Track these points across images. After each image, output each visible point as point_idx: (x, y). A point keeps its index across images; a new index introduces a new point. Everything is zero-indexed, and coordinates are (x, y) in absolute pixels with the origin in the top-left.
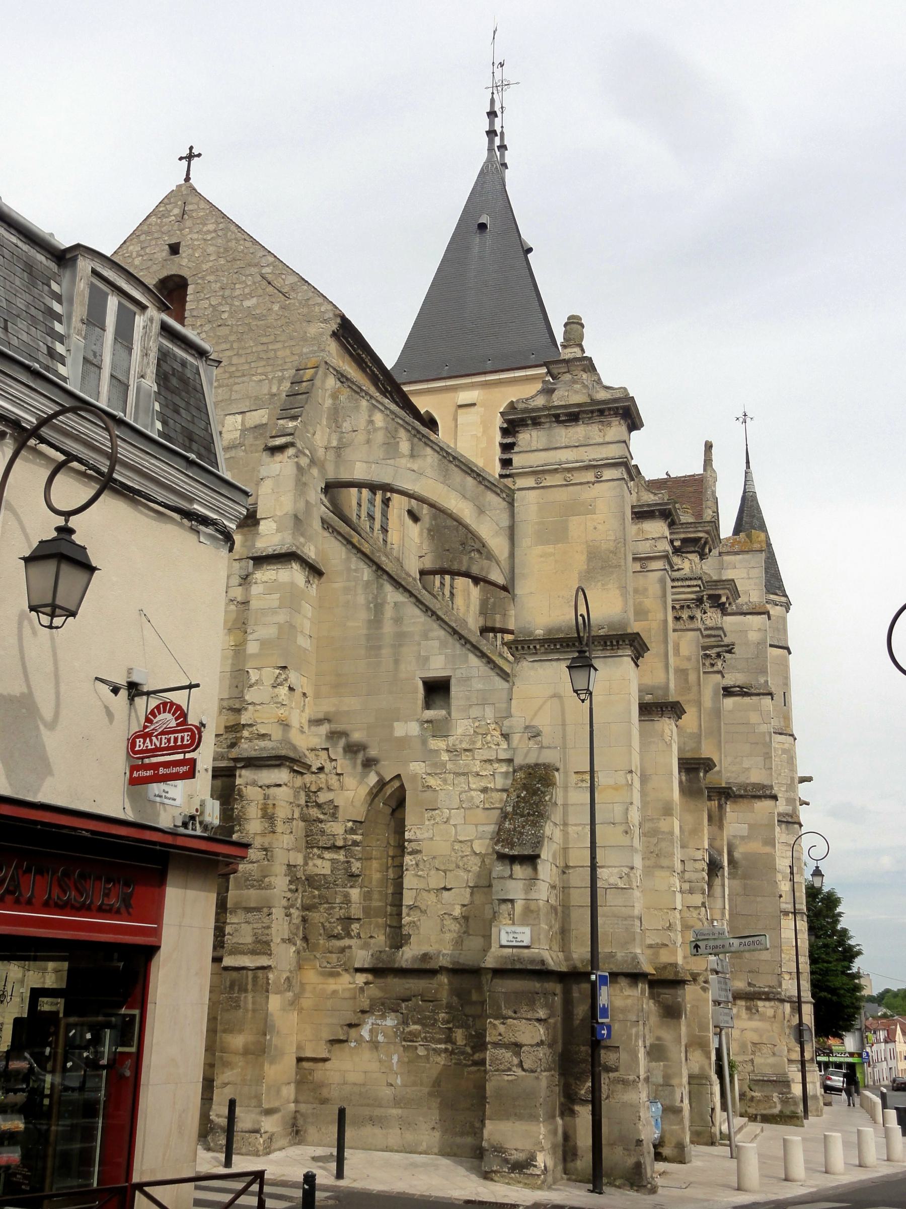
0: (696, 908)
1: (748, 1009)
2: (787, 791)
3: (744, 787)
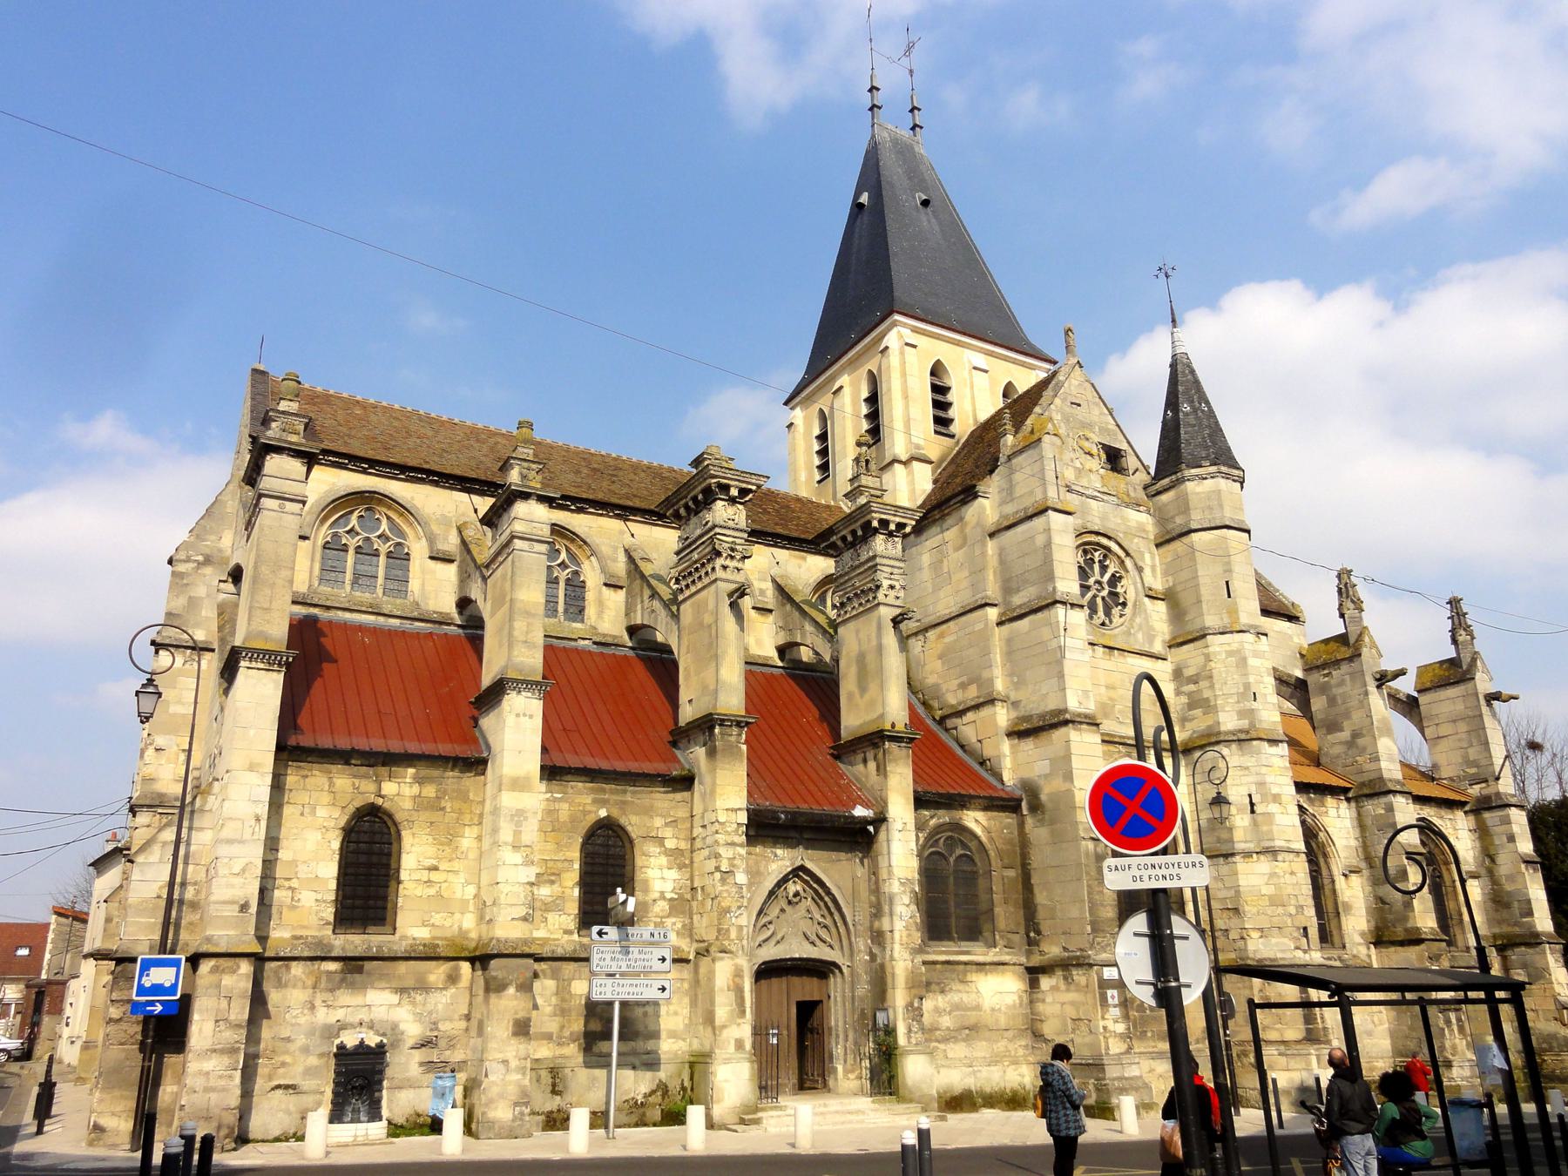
1: (1065, 978)
3: (1042, 716)
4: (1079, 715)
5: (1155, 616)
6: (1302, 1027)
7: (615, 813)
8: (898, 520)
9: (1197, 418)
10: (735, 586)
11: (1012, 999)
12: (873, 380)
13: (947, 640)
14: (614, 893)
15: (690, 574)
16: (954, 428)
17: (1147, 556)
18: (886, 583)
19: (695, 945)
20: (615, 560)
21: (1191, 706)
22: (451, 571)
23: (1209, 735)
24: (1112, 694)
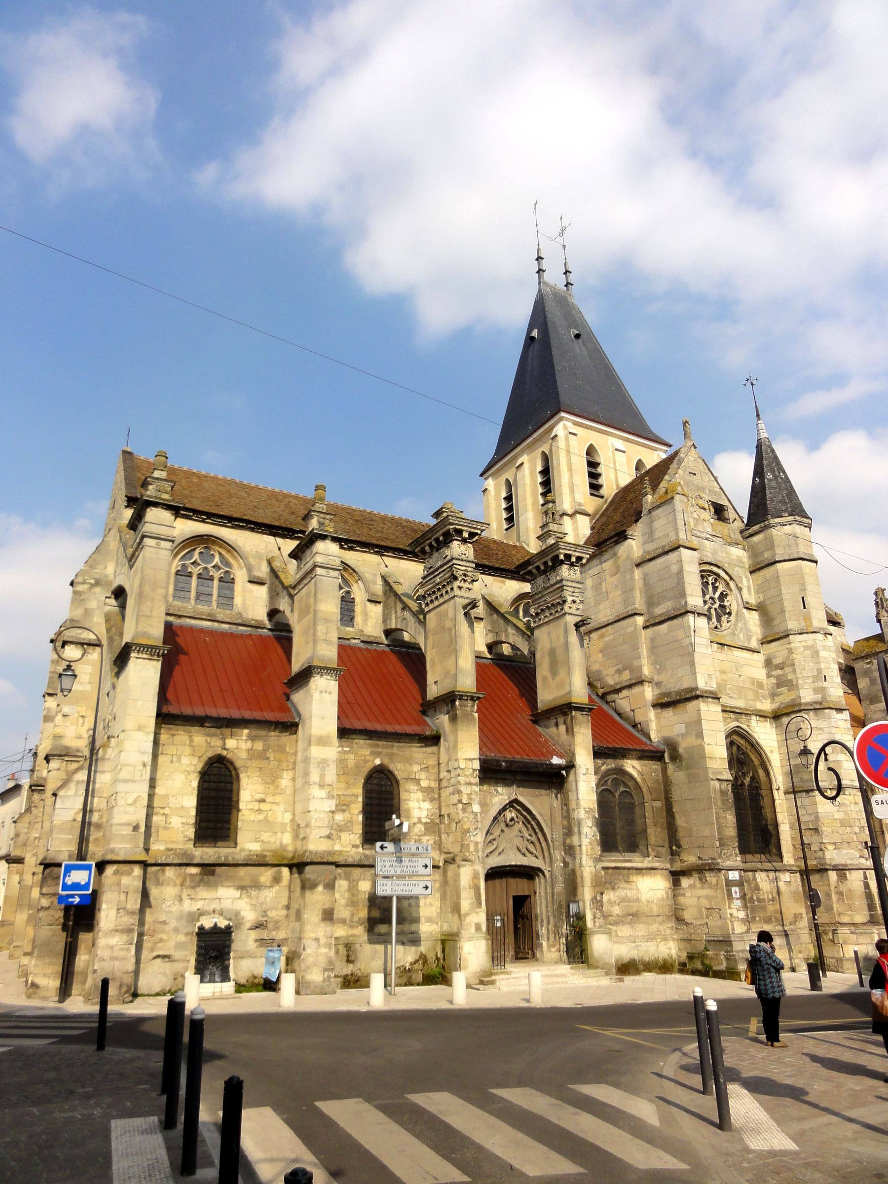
0: (456, 804)
1: (700, 879)
2: (814, 682)
3: (679, 693)
4: (706, 692)
5: (751, 622)
6: (867, 913)
7: (386, 761)
8: (577, 554)
9: (778, 483)
10: (467, 601)
11: (661, 894)
12: (546, 459)
13: (606, 639)
14: (391, 819)
15: (434, 592)
16: (602, 492)
17: (744, 580)
18: (570, 599)
19: (443, 856)
20: (375, 583)
21: (779, 685)
22: (262, 592)
23: (794, 706)
24: (725, 677)
